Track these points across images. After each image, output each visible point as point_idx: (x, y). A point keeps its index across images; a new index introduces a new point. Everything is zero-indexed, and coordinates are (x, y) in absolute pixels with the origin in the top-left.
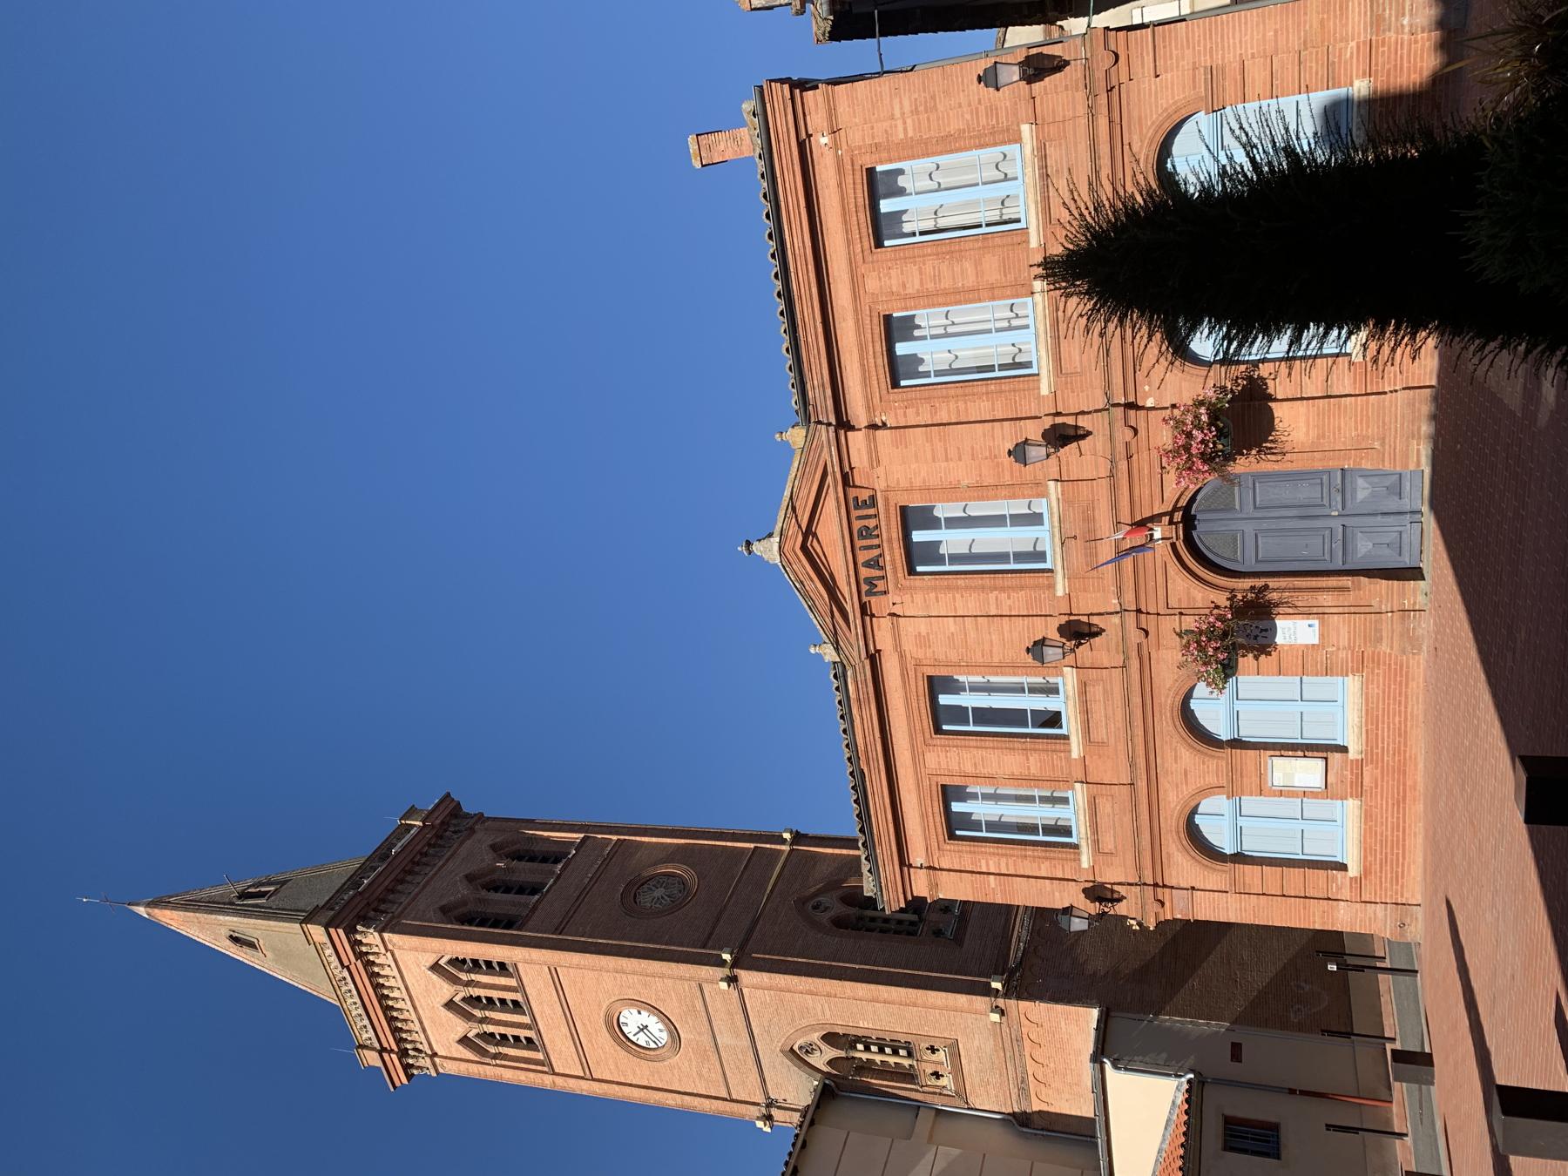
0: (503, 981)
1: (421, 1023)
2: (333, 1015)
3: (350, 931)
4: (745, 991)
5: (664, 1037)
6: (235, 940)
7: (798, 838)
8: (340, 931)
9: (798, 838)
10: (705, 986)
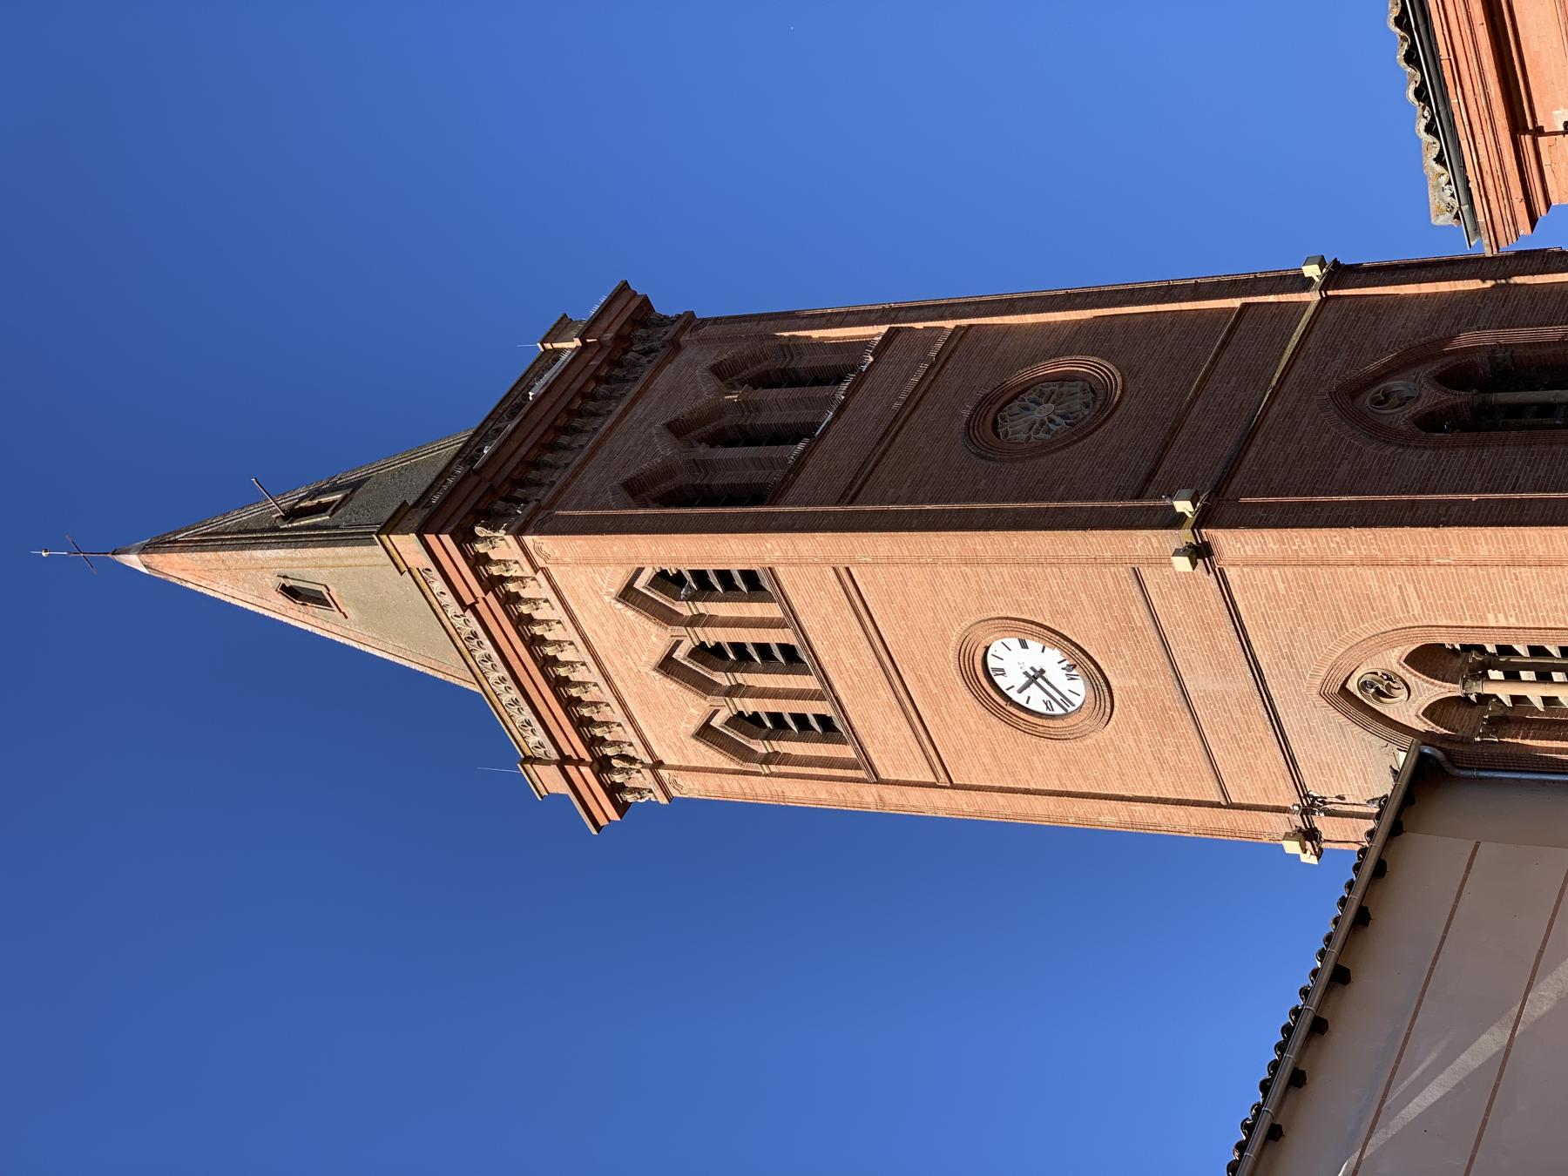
0: (756, 610)
1: (623, 705)
2: (471, 711)
3: (464, 538)
4: (1231, 574)
5: (1077, 690)
6: (291, 593)
7: (1338, 274)
8: (446, 538)
9: (1338, 274)
10: (1146, 573)
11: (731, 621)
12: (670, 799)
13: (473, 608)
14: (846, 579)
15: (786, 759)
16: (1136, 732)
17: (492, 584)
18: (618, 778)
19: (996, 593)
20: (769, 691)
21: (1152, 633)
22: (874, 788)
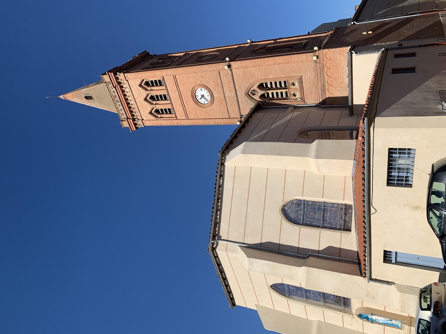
0: (161, 88)
1: (138, 108)
2: (115, 117)
3: (115, 74)
4: (233, 71)
5: (209, 98)
6: (87, 98)
7: (252, 42)
8: (112, 73)
9: (252, 42)
10: (221, 72)
11: (157, 91)
12: (144, 126)
13: (115, 87)
14: (175, 77)
15: (163, 117)
16: (217, 106)
17: (119, 83)
18: (136, 122)
19: (198, 79)
20: (161, 105)
21: (221, 85)
22: (176, 121)
